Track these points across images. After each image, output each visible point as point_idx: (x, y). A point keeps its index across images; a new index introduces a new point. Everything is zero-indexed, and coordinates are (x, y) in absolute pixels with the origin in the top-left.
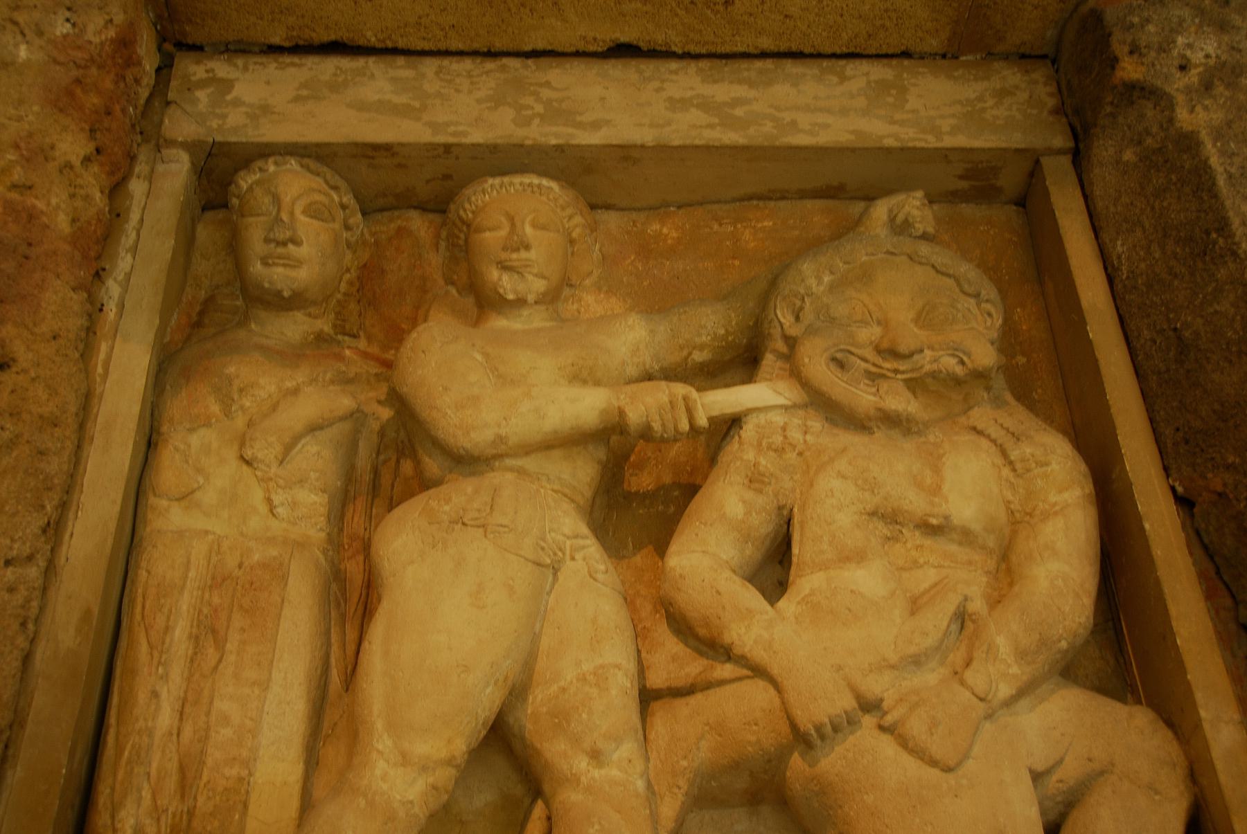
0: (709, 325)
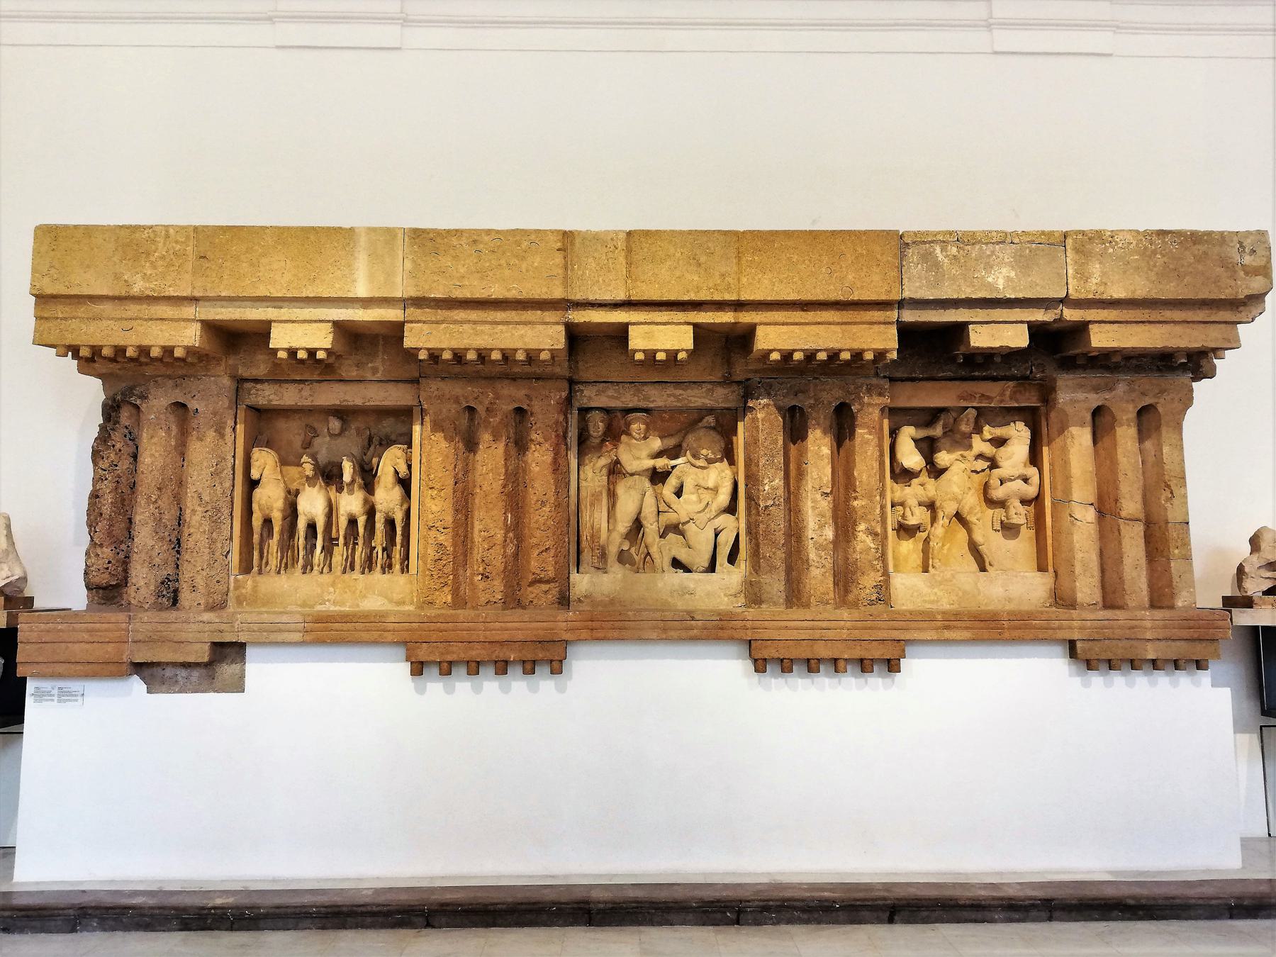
0: (671, 442)
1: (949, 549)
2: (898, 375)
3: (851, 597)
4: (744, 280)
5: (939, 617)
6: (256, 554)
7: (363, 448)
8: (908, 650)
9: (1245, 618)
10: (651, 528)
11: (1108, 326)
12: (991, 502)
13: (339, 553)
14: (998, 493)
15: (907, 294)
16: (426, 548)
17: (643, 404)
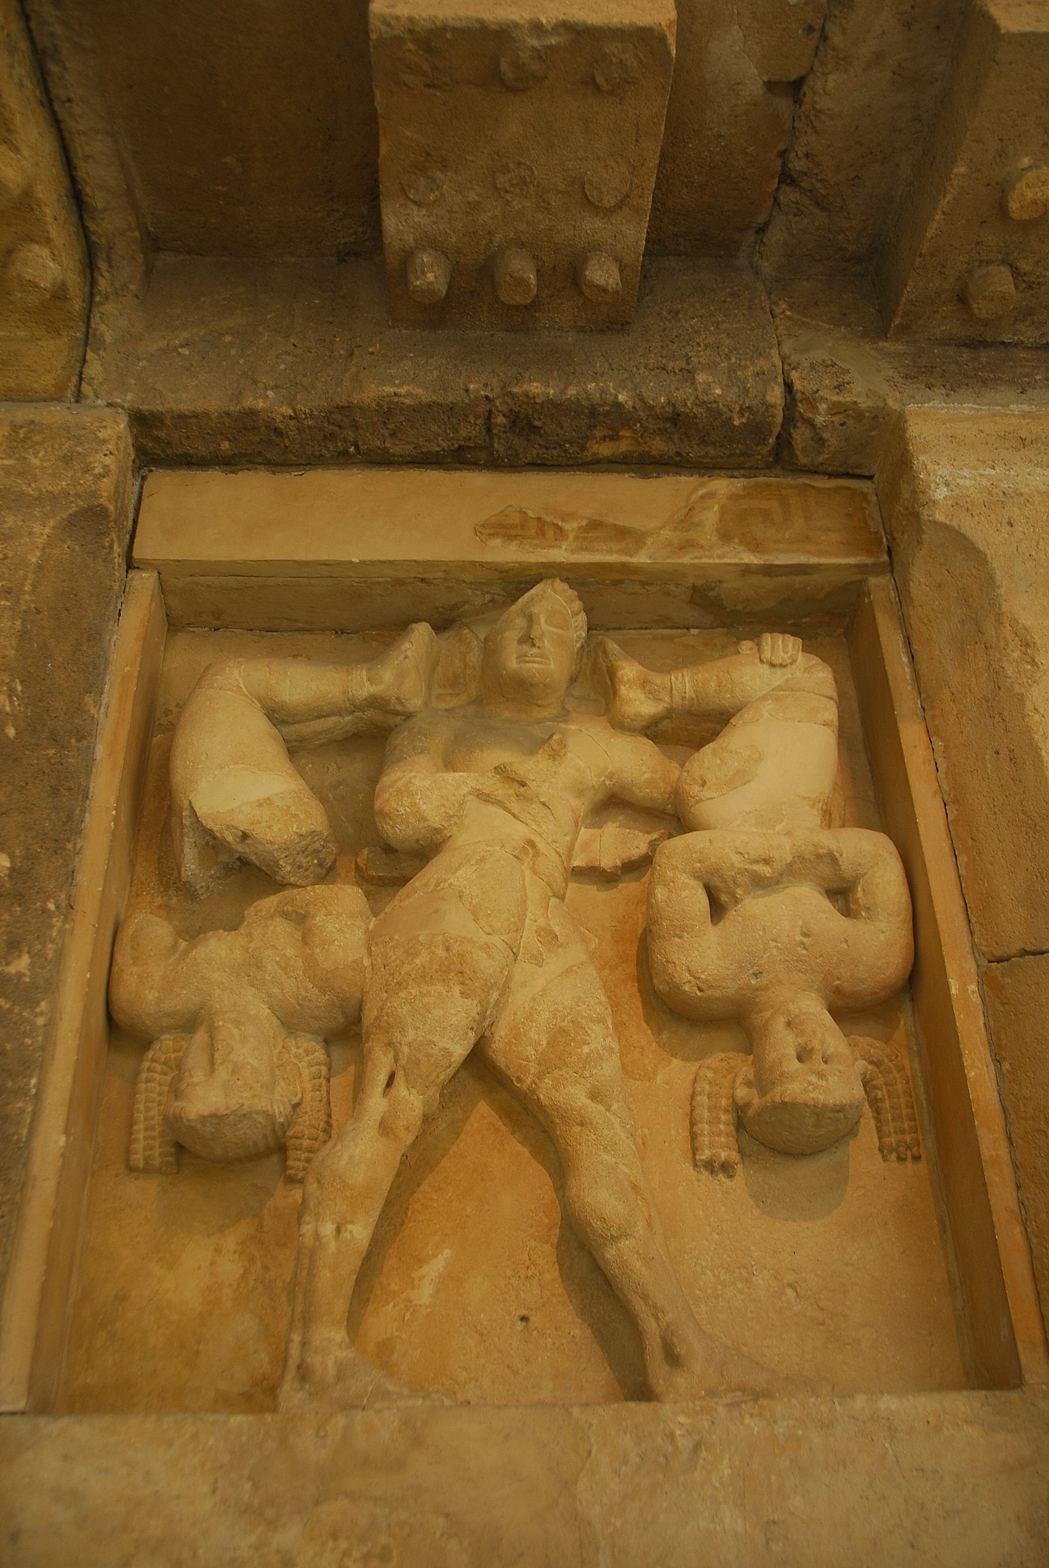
14: (702, 957)
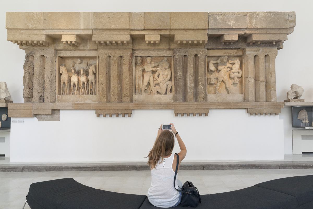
0: (156, 64)
1: (221, 89)
2: (210, 48)
3: (198, 100)
4: (172, 24)
5: (217, 103)
6: (62, 90)
7: (86, 66)
8: (210, 111)
9: (288, 104)
10: (152, 84)
11: (257, 35)
12: (230, 78)
13: (82, 91)
14: (232, 76)
15: (210, 27)
16: (100, 89)
17: (150, 55)
